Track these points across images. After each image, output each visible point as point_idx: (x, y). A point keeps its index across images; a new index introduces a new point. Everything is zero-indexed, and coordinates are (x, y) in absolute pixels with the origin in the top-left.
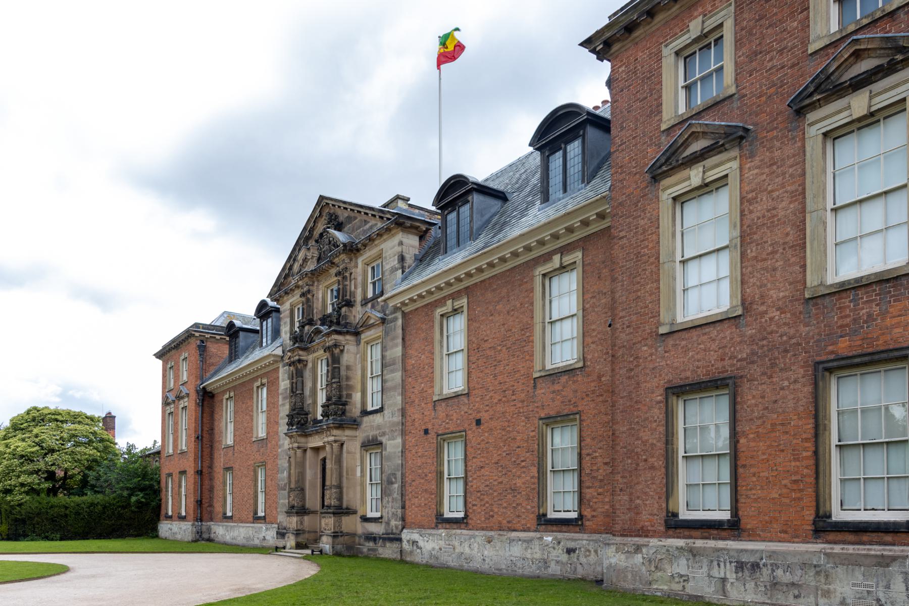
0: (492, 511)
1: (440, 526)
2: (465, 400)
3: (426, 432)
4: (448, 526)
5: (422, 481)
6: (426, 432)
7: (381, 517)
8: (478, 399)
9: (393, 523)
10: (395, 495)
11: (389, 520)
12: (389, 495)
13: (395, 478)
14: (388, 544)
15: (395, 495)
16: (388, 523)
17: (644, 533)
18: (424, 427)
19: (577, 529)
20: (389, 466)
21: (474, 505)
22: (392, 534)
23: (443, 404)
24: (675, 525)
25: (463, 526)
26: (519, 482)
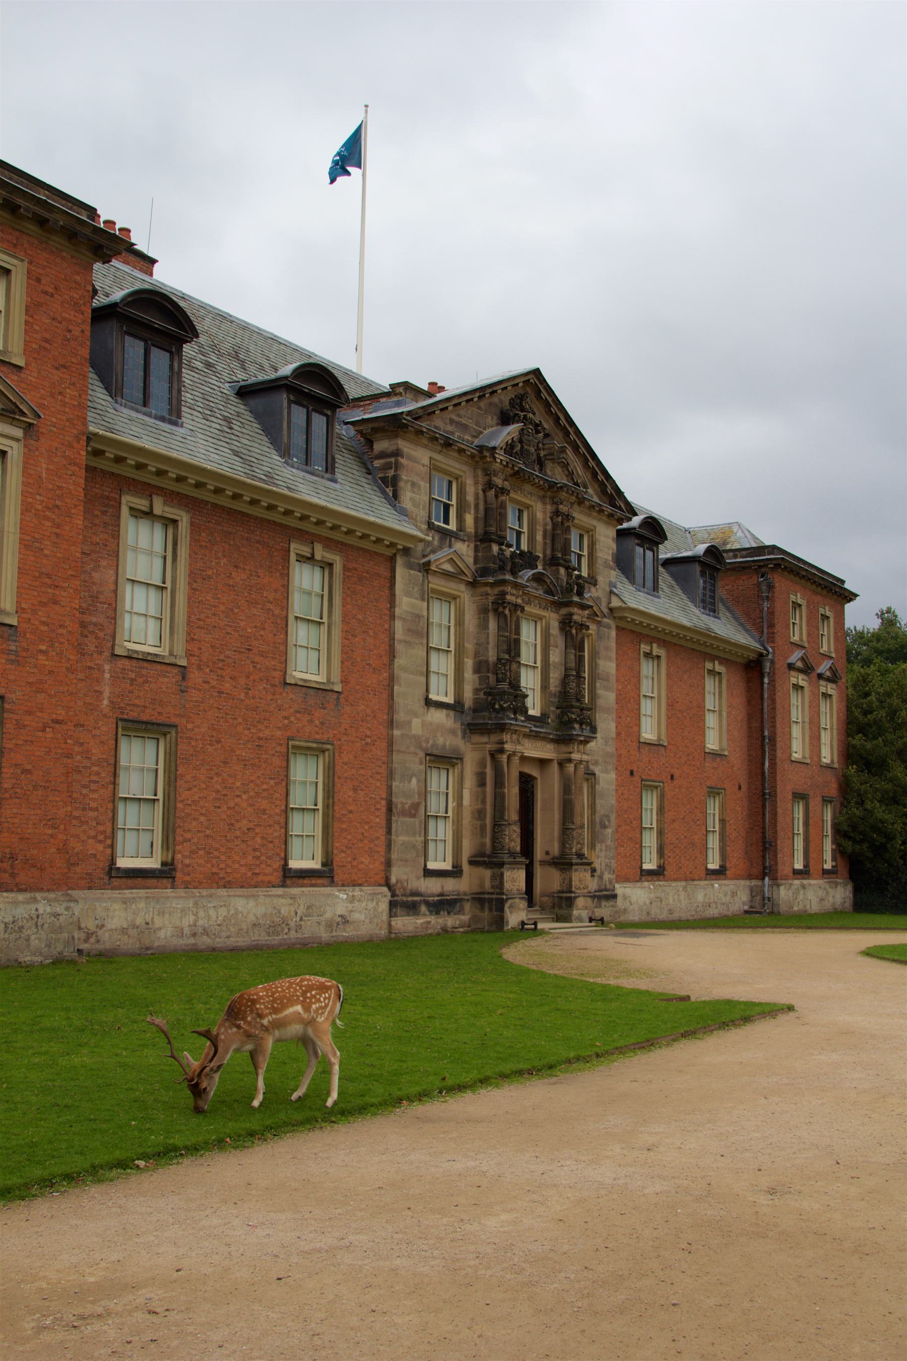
0: (680, 862)
1: (643, 878)
3: (632, 773)
4: (650, 878)
5: (628, 828)
6: (632, 773)
8: (672, 755)
9: (607, 876)
10: (609, 842)
11: (602, 874)
12: (602, 842)
14: (604, 903)
16: (601, 877)
18: (629, 768)
19: (723, 877)
21: (669, 857)
22: (606, 890)
23: (647, 748)
25: (661, 877)
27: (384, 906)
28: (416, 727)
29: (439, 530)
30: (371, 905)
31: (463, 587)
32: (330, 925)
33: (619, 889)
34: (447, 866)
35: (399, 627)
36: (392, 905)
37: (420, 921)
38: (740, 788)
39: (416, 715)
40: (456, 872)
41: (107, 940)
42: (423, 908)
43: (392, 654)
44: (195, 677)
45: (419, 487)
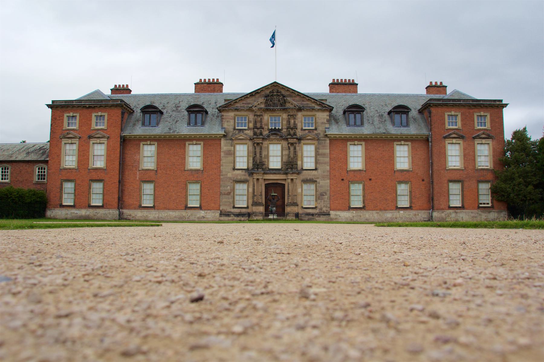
2: (364, 172)
7: (316, 207)
13: (326, 194)
15: (326, 200)
16: (321, 209)
17: (443, 209)
20: (320, 190)
24: (450, 208)
26: (388, 198)
27: (218, 214)
28: (229, 175)
29: (237, 129)
30: (213, 214)
31: (248, 141)
32: (198, 218)
33: (332, 213)
34: (246, 206)
35: (222, 154)
36: (221, 214)
37: (230, 218)
38: (423, 180)
39: (229, 172)
40: (248, 207)
41: (137, 218)
42: (232, 215)
43: (220, 160)
44: (159, 171)
45: (230, 122)
